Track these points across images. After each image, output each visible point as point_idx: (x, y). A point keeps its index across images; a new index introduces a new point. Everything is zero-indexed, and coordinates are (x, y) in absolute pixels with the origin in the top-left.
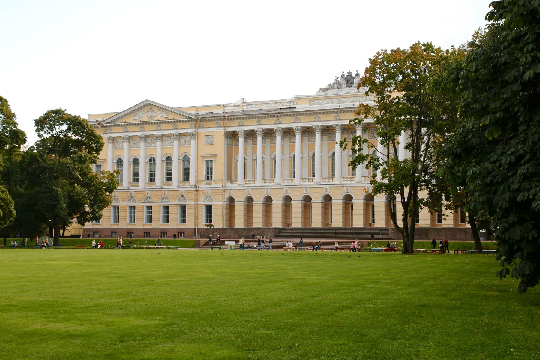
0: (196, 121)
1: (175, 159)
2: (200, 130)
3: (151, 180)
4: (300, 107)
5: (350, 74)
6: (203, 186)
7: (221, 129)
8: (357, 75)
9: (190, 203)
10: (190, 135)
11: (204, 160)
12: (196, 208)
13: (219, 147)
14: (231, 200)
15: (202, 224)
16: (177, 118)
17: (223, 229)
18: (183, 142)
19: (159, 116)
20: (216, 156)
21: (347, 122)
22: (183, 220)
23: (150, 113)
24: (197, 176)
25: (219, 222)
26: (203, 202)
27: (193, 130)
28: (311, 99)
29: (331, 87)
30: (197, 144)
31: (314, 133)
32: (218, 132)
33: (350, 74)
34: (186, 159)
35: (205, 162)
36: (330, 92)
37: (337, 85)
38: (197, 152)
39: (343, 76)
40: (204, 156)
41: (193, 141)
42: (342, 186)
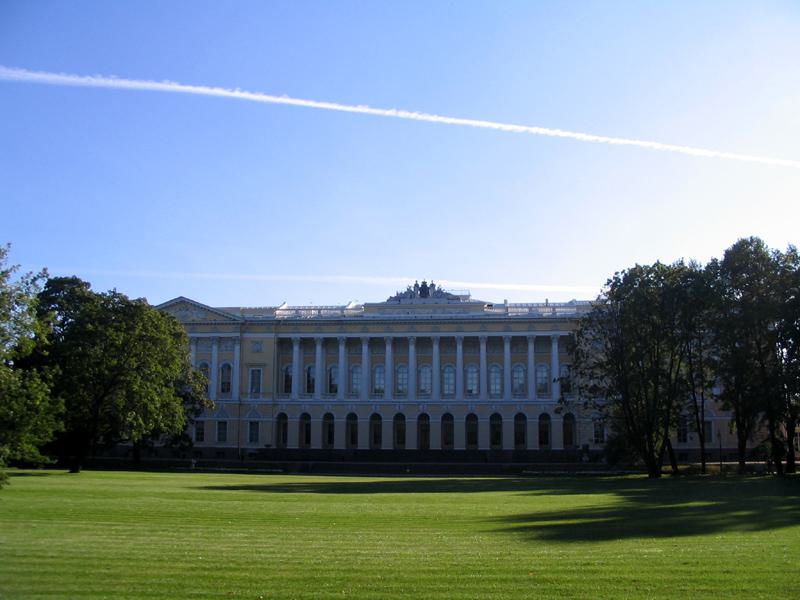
0: (242, 324)
1: (236, 368)
2: (246, 335)
3: (223, 391)
5: (424, 284)
6: (248, 399)
7: (272, 335)
8: (433, 285)
10: (233, 340)
11: (250, 369)
14: (283, 417)
16: (219, 319)
17: (296, 450)
18: (223, 347)
20: (265, 365)
21: (566, 333)
22: (222, 437)
23: (184, 313)
24: (241, 388)
27: (238, 334)
31: (315, 345)
33: (424, 284)
34: (226, 368)
35: (250, 372)
37: (409, 294)
38: (241, 359)
39: (416, 285)
40: (252, 365)
41: (237, 347)
42: (419, 404)
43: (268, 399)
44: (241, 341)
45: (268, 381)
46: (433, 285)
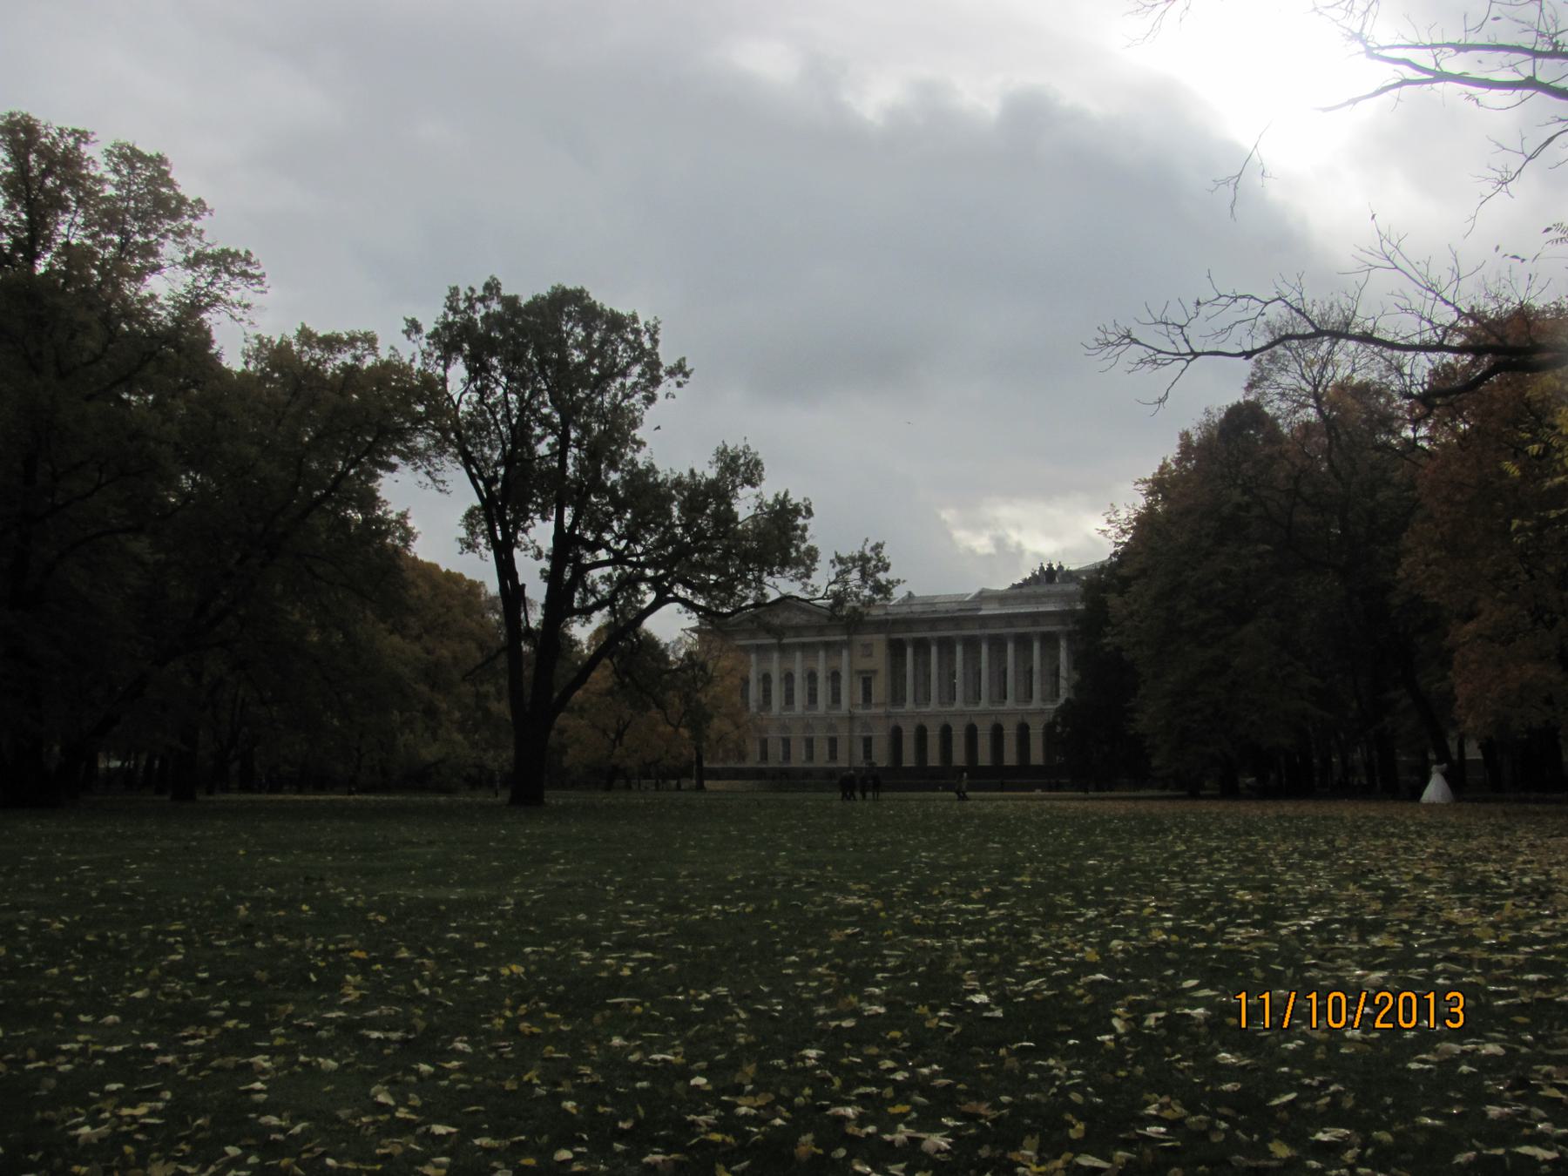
2: (855, 637)
4: (987, 610)
6: (859, 711)
7: (882, 636)
8: (1060, 567)
9: (842, 732)
12: (851, 742)
13: (879, 660)
15: (859, 761)
19: (799, 619)
20: (875, 672)
22: (833, 755)
24: (851, 698)
25: (881, 759)
26: (858, 732)
28: (1002, 598)
29: (1026, 582)
30: (850, 655)
32: (879, 642)
36: (1025, 590)
40: (860, 672)
41: (845, 653)
43: (880, 711)
44: (847, 644)
45: (880, 688)
46: (1060, 567)
